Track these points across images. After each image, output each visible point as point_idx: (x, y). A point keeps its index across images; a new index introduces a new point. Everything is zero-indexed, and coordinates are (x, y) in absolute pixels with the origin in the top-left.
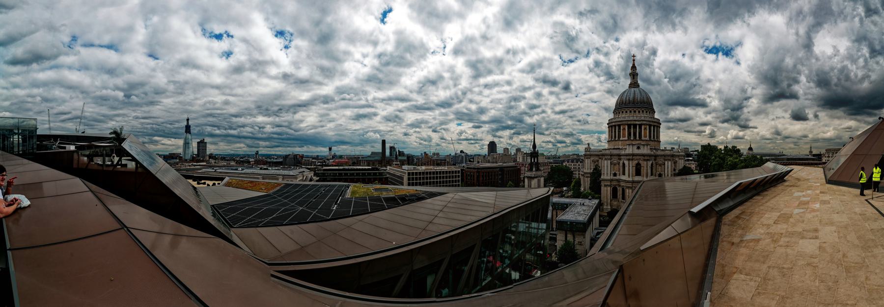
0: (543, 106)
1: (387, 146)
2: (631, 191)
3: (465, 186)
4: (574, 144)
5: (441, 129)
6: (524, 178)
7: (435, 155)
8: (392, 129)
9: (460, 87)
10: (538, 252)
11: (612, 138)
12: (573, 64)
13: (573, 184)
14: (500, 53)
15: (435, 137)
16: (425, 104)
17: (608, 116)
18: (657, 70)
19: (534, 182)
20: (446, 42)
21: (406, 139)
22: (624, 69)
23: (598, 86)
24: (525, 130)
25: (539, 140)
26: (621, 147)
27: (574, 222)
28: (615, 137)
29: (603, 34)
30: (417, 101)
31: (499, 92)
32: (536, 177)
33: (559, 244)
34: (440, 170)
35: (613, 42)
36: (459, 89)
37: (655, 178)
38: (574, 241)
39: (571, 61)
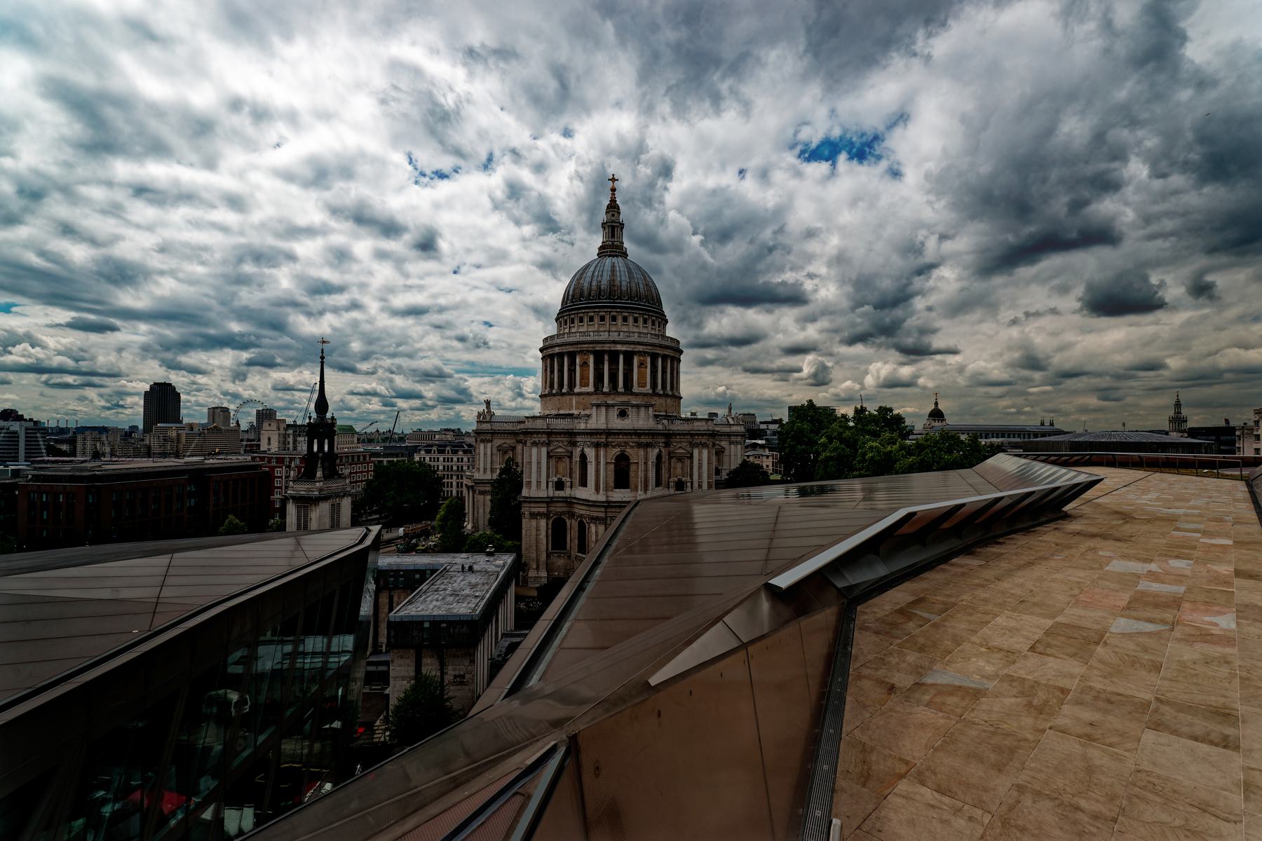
0: (355, 289)
2: (601, 528)
3: (20, 550)
4: (446, 401)
11: (552, 386)
12: (445, 181)
13: (442, 512)
17: (545, 329)
18: (672, 215)
19: (319, 514)
23: (515, 249)
24: (292, 354)
25: (338, 387)
26: (575, 412)
28: (561, 385)
29: (531, 113)
31: (197, 224)
32: (326, 498)
33: (397, 689)
35: (556, 138)
38: (443, 674)
39: (441, 175)
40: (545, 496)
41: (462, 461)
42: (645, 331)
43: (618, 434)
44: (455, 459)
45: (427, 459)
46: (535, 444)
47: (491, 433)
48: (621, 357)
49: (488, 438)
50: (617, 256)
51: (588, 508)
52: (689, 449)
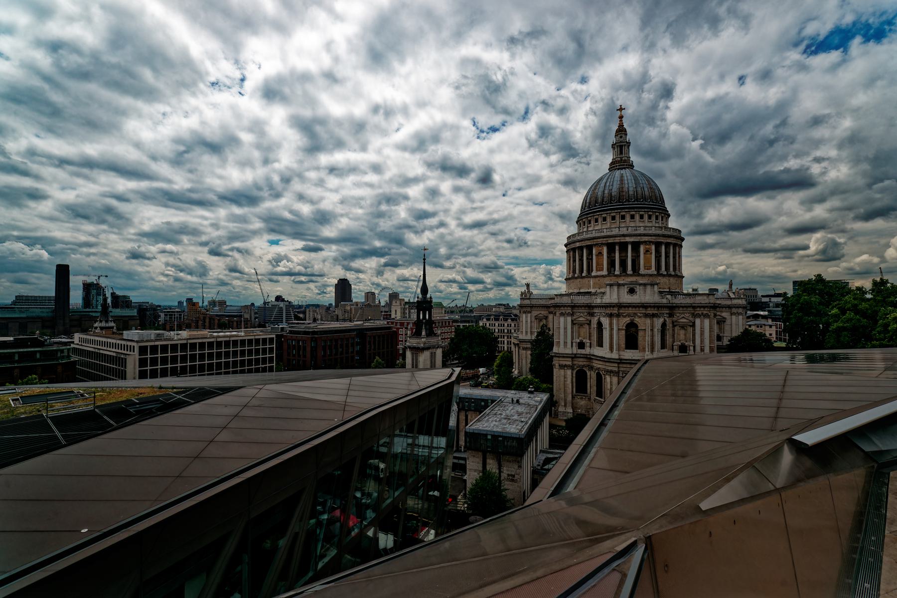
0: (441, 214)
1: (76, 282)
2: (615, 379)
3: (285, 370)
4: (499, 285)
5: (232, 249)
6: (404, 349)
7: (215, 306)
8: (92, 239)
9: (276, 165)
10: (431, 493)
11: (574, 272)
12: (497, 134)
13: (497, 361)
14: (359, 110)
15: (217, 266)
16: (191, 190)
17: (567, 230)
18: (674, 127)
19: (424, 357)
20: (245, 69)
21: (137, 267)
22: (600, 136)
23: (545, 173)
24: (407, 258)
25: (434, 277)
26: (593, 291)
27: (500, 436)
28: (581, 271)
29: (556, 73)
30: (170, 181)
31: (357, 185)
32: (428, 349)
33: (472, 476)
34: (228, 339)
36: (274, 171)
37: (670, 354)
38: (500, 472)
39: (494, 130)
40: (571, 353)
41: (511, 326)
42: (650, 225)
43: (628, 307)
44: (506, 325)
45: (488, 324)
46: (562, 314)
47: (530, 307)
49: (528, 310)
50: (625, 168)
51: (604, 363)
52: (691, 319)
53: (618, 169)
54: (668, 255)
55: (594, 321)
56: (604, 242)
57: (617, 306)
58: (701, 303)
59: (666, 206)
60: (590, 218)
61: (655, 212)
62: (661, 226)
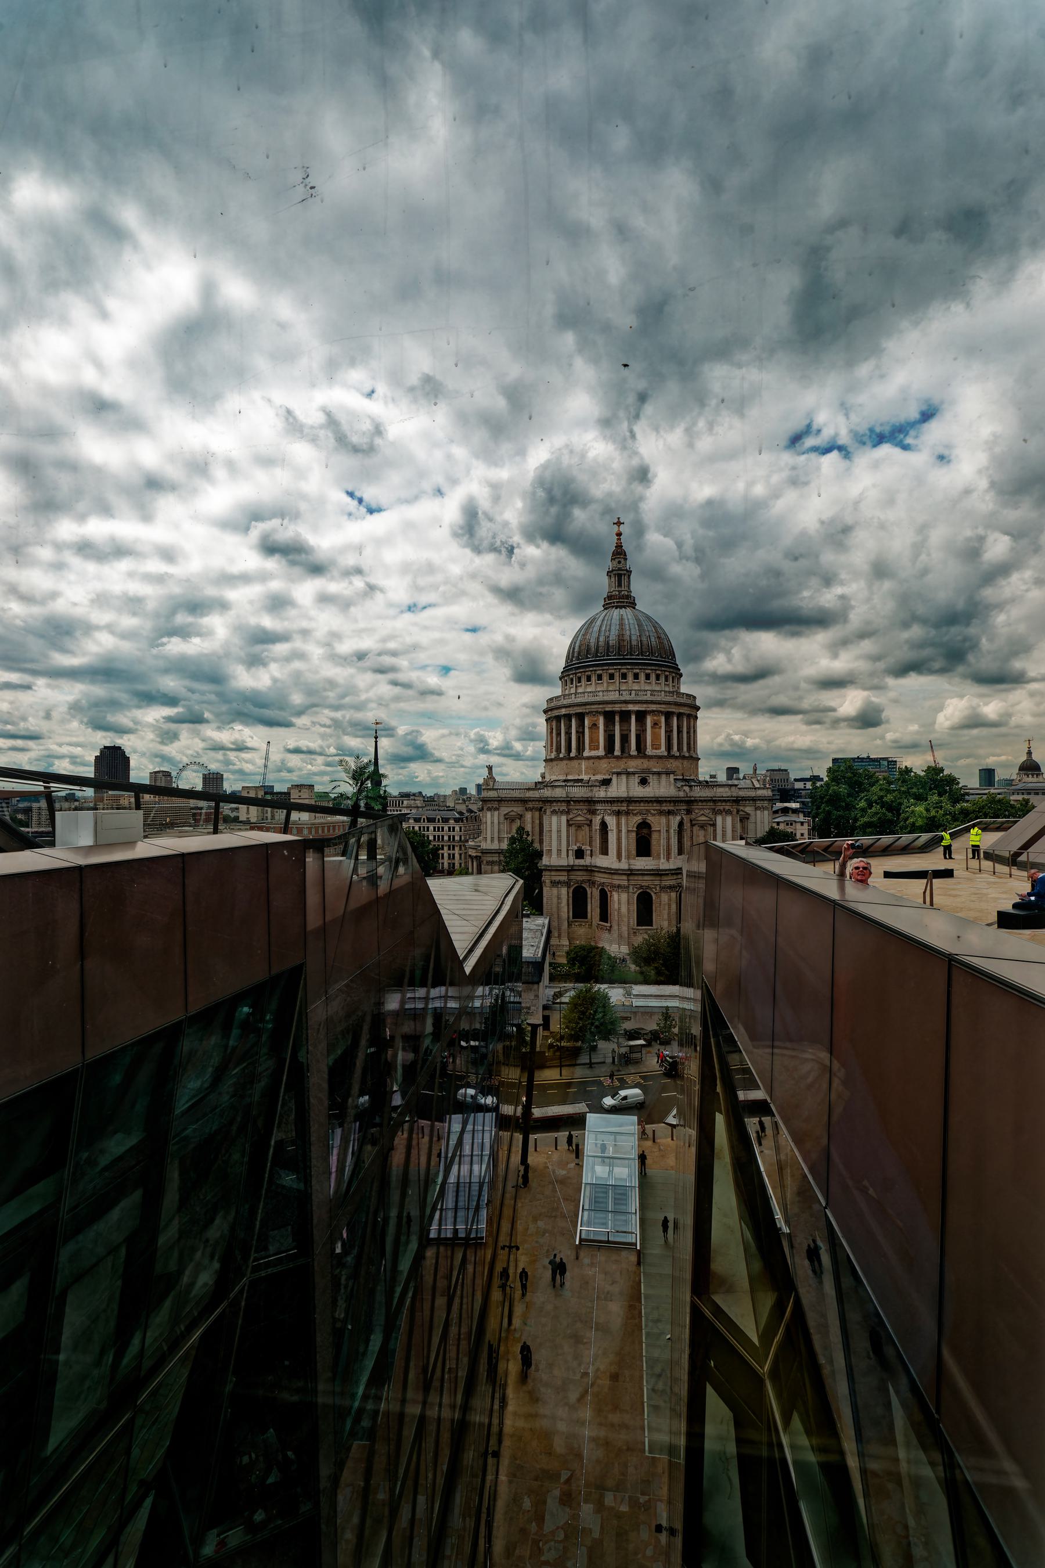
11: (558, 750)
26: (585, 777)
41: (454, 831)
42: (658, 688)
43: (640, 802)
44: (446, 828)
45: (417, 828)
46: (554, 812)
48: (633, 718)
49: (495, 806)
50: (624, 607)
52: (712, 816)
53: (617, 607)
54: (681, 729)
55: (597, 820)
56: (600, 710)
57: (626, 801)
58: (722, 797)
59: (677, 663)
60: (580, 675)
61: (665, 671)
62: (671, 690)
